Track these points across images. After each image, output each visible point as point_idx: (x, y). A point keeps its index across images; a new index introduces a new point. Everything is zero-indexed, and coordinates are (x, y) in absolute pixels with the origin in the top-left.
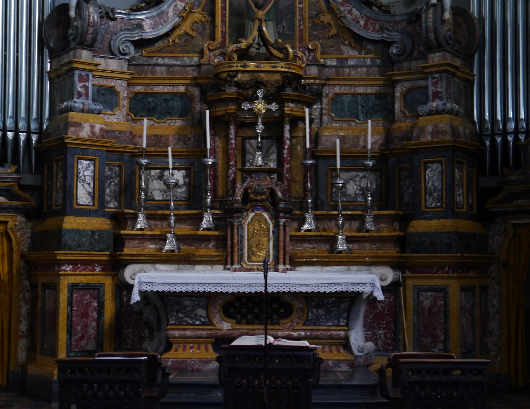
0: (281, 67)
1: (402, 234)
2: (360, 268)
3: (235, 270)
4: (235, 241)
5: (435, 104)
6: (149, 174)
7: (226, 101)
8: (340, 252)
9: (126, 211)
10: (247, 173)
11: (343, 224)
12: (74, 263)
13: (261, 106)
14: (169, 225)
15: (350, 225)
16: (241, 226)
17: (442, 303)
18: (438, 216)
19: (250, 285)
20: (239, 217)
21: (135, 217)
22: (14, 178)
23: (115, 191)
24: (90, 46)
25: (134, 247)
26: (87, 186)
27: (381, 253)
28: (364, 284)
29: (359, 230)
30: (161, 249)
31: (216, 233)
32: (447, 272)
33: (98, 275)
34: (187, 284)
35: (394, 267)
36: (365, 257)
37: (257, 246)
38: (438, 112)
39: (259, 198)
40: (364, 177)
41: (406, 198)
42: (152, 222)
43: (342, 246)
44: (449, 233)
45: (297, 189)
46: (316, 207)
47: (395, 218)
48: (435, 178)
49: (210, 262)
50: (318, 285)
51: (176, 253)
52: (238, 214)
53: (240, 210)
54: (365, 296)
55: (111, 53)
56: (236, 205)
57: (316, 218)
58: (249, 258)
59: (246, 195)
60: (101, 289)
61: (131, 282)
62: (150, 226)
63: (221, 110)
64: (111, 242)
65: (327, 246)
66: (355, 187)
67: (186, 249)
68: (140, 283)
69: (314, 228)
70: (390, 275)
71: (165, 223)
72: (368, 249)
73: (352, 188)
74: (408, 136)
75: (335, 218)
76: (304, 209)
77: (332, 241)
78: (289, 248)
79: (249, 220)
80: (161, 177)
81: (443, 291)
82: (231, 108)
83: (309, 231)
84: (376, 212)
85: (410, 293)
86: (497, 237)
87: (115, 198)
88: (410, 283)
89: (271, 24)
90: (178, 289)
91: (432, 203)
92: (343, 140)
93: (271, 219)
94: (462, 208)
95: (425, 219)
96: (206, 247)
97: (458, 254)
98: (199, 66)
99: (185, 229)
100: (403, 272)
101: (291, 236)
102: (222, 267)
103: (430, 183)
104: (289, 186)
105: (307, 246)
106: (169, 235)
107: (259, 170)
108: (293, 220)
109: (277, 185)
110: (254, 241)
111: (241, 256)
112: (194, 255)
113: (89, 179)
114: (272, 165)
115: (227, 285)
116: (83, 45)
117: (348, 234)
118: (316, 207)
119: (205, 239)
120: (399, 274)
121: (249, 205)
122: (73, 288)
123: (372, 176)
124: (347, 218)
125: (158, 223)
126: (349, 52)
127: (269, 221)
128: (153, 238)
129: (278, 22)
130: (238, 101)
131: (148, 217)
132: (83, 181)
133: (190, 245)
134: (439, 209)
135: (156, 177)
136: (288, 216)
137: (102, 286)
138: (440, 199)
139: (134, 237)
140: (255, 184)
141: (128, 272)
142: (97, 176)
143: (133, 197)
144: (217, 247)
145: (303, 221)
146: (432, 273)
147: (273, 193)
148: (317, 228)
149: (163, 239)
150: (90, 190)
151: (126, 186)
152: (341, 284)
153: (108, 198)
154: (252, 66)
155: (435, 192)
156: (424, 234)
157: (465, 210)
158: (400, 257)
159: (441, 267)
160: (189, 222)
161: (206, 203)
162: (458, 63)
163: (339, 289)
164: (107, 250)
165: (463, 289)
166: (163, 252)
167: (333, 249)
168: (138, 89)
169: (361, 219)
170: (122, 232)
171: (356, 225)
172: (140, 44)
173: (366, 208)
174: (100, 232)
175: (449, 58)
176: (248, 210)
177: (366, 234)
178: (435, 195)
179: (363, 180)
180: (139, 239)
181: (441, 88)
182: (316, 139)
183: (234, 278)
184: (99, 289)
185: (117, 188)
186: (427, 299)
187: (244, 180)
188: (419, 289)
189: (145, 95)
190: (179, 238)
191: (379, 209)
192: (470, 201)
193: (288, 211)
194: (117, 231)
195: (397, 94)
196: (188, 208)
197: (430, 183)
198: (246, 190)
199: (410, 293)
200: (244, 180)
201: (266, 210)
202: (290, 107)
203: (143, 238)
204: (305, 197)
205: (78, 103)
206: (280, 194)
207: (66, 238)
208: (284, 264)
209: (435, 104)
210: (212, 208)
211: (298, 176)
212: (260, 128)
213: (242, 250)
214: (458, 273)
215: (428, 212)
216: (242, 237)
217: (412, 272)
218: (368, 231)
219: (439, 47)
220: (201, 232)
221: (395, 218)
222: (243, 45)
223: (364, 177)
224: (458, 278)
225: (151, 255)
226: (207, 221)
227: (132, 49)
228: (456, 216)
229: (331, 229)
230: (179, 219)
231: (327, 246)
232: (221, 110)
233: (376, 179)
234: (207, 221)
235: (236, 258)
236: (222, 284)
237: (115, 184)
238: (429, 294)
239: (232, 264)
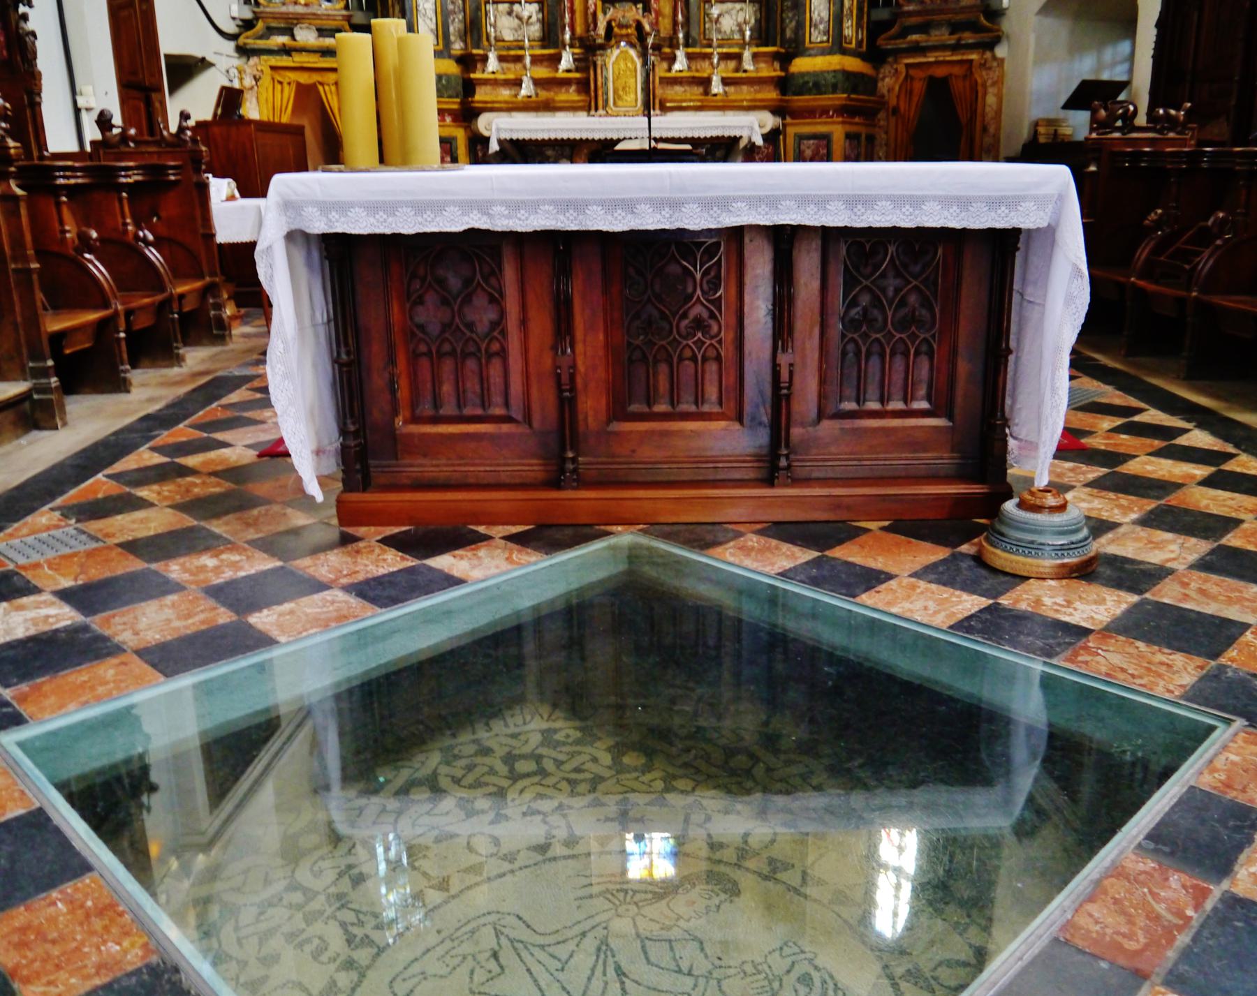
1: (783, 74)
2: (737, 113)
3: (600, 116)
4: (599, 83)
6: (497, 9)
8: (715, 95)
9: (475, 51)
11: (718, 63)
14: (525, 67)
15: (726, 65)
16: (604, 65)
17: (825, 151)
18: (824, 52)
19: (618, 130)
20: (602, 55)
21: (485, 59)
22: (343, 16)
23: (459, 30)
25: (486, 94)
26: (428, 22)
27: (759, 96)
28: (742, 127)
29: (737, 70)
30: (516, 96)
31: (577, 75)
32: (832, 117)
33: (449, 126)
34: (549, 130)
36: (742, 101)
37: (624, 88)
39: (624, 32)
40: (741, 9)
41: (789, 33)
42: (505, 65)
43: (717, 88)
44: (835, 71)
45: (665, 25)
46: (687, 45)
47: (775, 56)
48: (822, 7)
49: (572, 108)
50: (692, 129)
51: (534, 98)
52: (601, 52)
53: (603, 47)
54: (742, 144)
56: (600, 41)
57: (690, 57)
58: (615, 103)
59: (609, 28)
60: (453, 143)
61: (486, 133)
62: (503, 69)
64: (460, 88)
65: (701, 90)
66: (731, 22)
67: (544, 95)
68: (498, 130)
69: (686, 67)
70: (769, 121)
71: (519, 66)
72: (746, 93)
73: (728, 24)
75: (708, 57)
76: (673, 44)
77: (706, 83)
78: (659, 92)
79: (613, 58)
80: (510, 13)
83: (681, 71)
84: (755, 49)
85: (790, 141)
86: (887, 80)
87: (461, 38)
88: (791, 131)
90: (540, 136)
93: (639, 57)
94: (851, 43)
95: (810, 55)
96: (567, 91)
97: (845, 95)
99: (543, 72)
100: (784, 118)
101: (661, 78)
102: (585, 113)
103: (816, 13)
104: (657, 18)
105: (678, 89)
106: (525, 79)
108: (663, 59)
109: (644, 16)
110: (620, 83)
111: (606, 102)
112: (554, 101)
113: (431, 14)
115: (593, 130)
117: (724, 75)
118: (687, 45)
120: (779, 121)
121: (613, 41)
124: (725, 57)
125: (511, 66)
127: (636, 59)
128: (507, 83)
131: (501, 59)
132: (424, 15)
133: (548, 90)
134: (825, 44)
135: (505, 12)
136: (656, 53)
137: (455, 139)
138: (827, 32)
139: (485, 82)
140: (619, 15)
142: (439, 10)
143: (480, 37)
144: (579, 92)
145: (672, 59)
146: (815, 117)
147: (639, 26)
148: (689, 68)
149: (518, 83)
150: (434, 27)
151: (472, 22)
152: (717, 128)
153: (452, 38)
155: (821, 23)
156: (808, 73)
157: (853, 45)
158: (781, 100)
159: (824, 112)
160: (545, 63)
161: (563, 41)
163: (715, 133)
164: (457, 97)
165: (848, 136)
166: (520, 98)
167: (707, 92)
169: (738, 57)
170: (472, 76)
171: (732, 64)
173: (743, 45)
174: (448, 77)
176: (612, 47)
177: (744, 75)
178: (821, 27)
179: (740, 13)
180: (491, 84)
183: (600, 123)
184: (451, 144)
185: (461, 26)
186: (808, 148)
187: (605, 13)
190: (537, 82)
191: (758, 46)
192: (860, 36)
194: (466, 76)
196: (543, 47)
197: (816, 13)
198: (609, 23)
199: (790, 141)
200: (605, 13)
201: (632, 45)
203: (495, 83)
204: (675, 32)
206: (647, 28)
208: (654, 109)
210: (572, 46)
213: (607, 94)
214: (843, 116)
215: (813, 49)
216: (606, 79)
217: (793, 117)
218: (745, 71)
220: (561, 74)
221: (775, 56)
223: (741, 9)
224: (843, 123)
225: (506, 102)
226: (567, 60)
228: (844, 52)
229: (704, 69)
230: (536, 60)
231: (701, 90)
233: (755, 12)
234: (567, 60)
235: (600, 103)
236: (587, 130)
237: (460, 21)
238: (811, 142)
239: (596, 109)
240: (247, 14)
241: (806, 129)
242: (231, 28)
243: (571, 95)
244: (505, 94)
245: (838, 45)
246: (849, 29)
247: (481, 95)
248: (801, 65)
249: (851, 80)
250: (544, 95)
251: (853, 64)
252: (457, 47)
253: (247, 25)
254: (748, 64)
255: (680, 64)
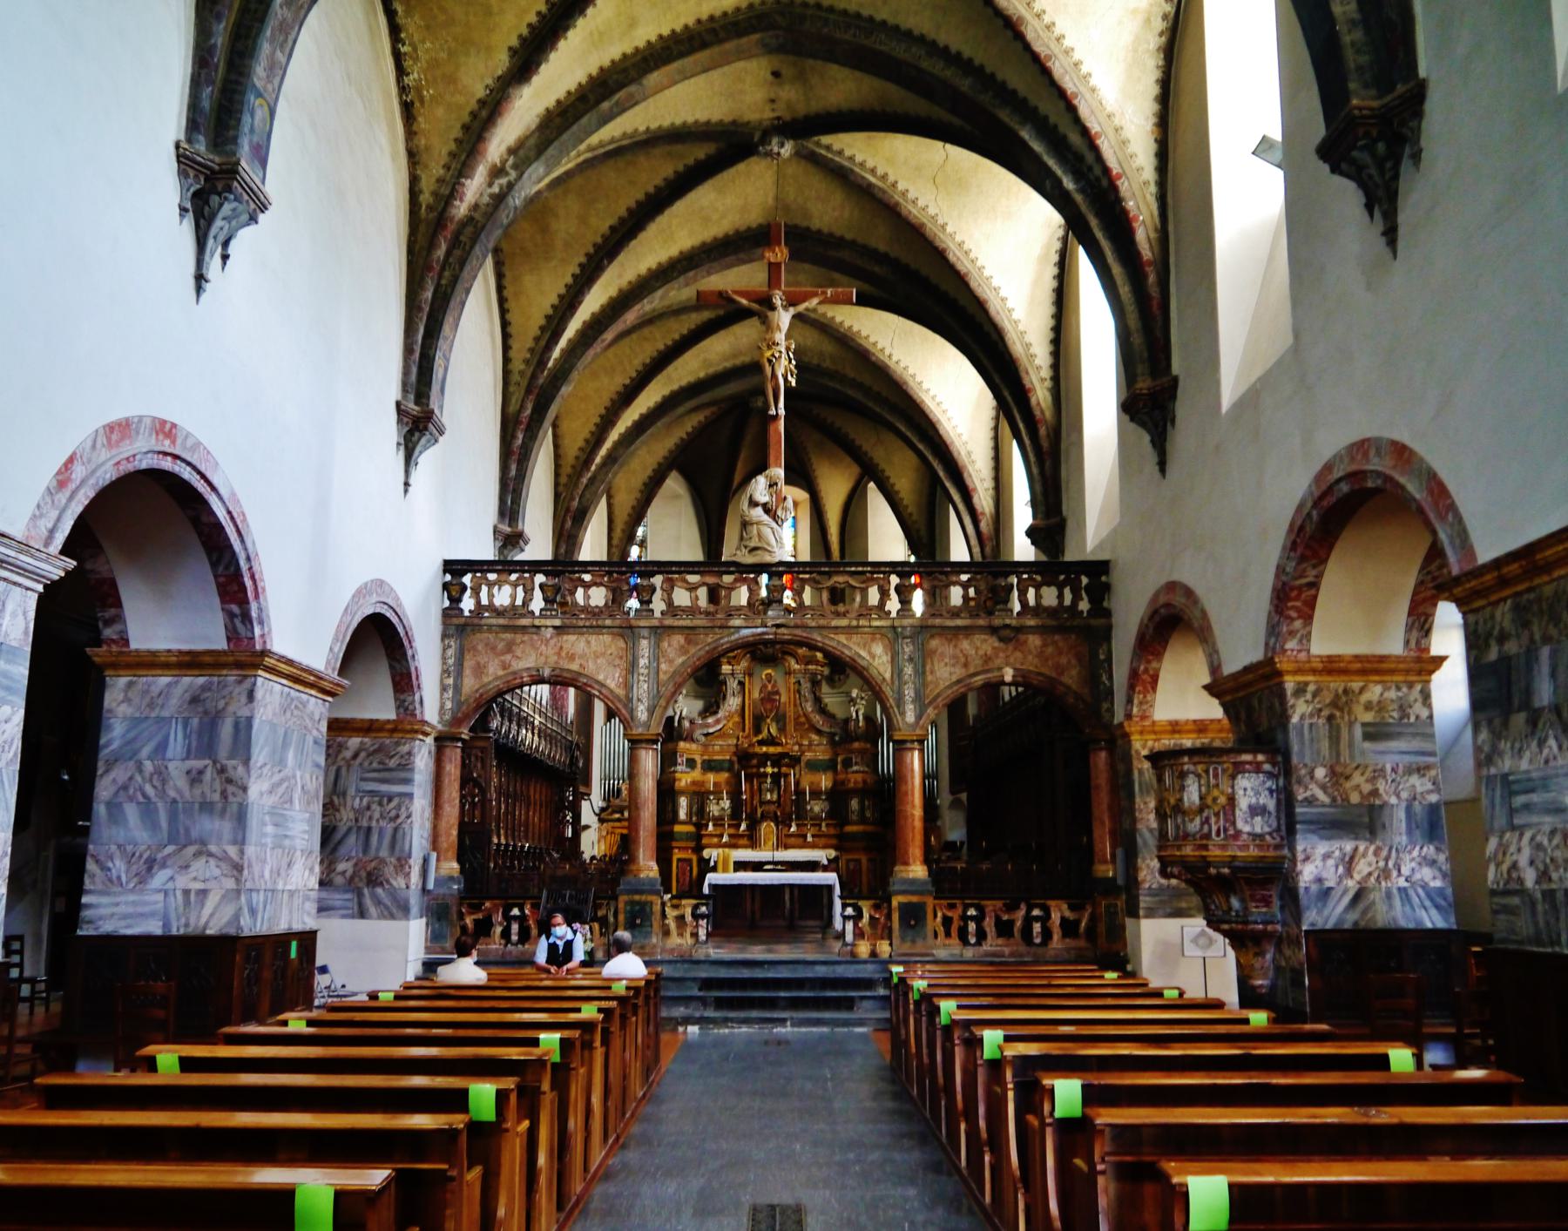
0: (779, 749)
5: (855, 768)
7: (753, 767)
10: (762, 803)
12: (679, 848)
13: (769, 770)
21: (707, 825)
24: (685, 740)
35: (836, 848)
38: (857, 772)
43: (809, 839)
49: (745, 847)
53: (760, 822)
55: (693, 740)
63: (749, 771)
67: (733, 841)
70: (832, 853)
72: (822, 841)
74: (843, 783)
76: (791, 820)
77: (805, 837)
81: (858, 861)
82: (754, 770)
89: (774, 725)
91: (854, 817)
92: (811, 784)
98: (737, 745)
99: (732, 831)
107: (770, 802)
114: (775, 797)
116: (681, 738)
118: (797, 819)
119: (742, 836)
122: (679, 860)
123: (826, 803)
126: (814, 737)
128: (716, 836)
129: (777, 722)
130: (758, 767)
141: (706, 853)
147: (775, 813)
154: (764, 749)
162: (869, 746)
165: (869, 860)
168: (706, 757)
169: (820, 825)
172: (706, 735)
175: (862, 744)
181: (859, 760)
182: (797, 783)
188: (848, 861)
189: (709, 761)
190: (730, 836)
193: (783, 822)
195: (839, 759)
202: (784, 770)
203: (711, 835)
205: (679, 768)
207: (676, 836)
209: (855, 768)
211: (789, 802)
212: (769, 780)
219: (857, 739)
222: (760, 737)
226: (743, 827)
227: (703, 739)
232: (749, 771)
234: (743, 827)
240: (604, 805)
241: (850, 857)
242: (597, 811)
243: (744, 841)
244: (715, 840)
245: (863, 820)
246: (868, 814)
247: (705, 841)
248: (850, 829)
249: (864, 836)
250: (733, 841)
251: (869, 828)
252: (694, 819)
253: (603, 810)
254: (824, 828)
255: (793, 829)
